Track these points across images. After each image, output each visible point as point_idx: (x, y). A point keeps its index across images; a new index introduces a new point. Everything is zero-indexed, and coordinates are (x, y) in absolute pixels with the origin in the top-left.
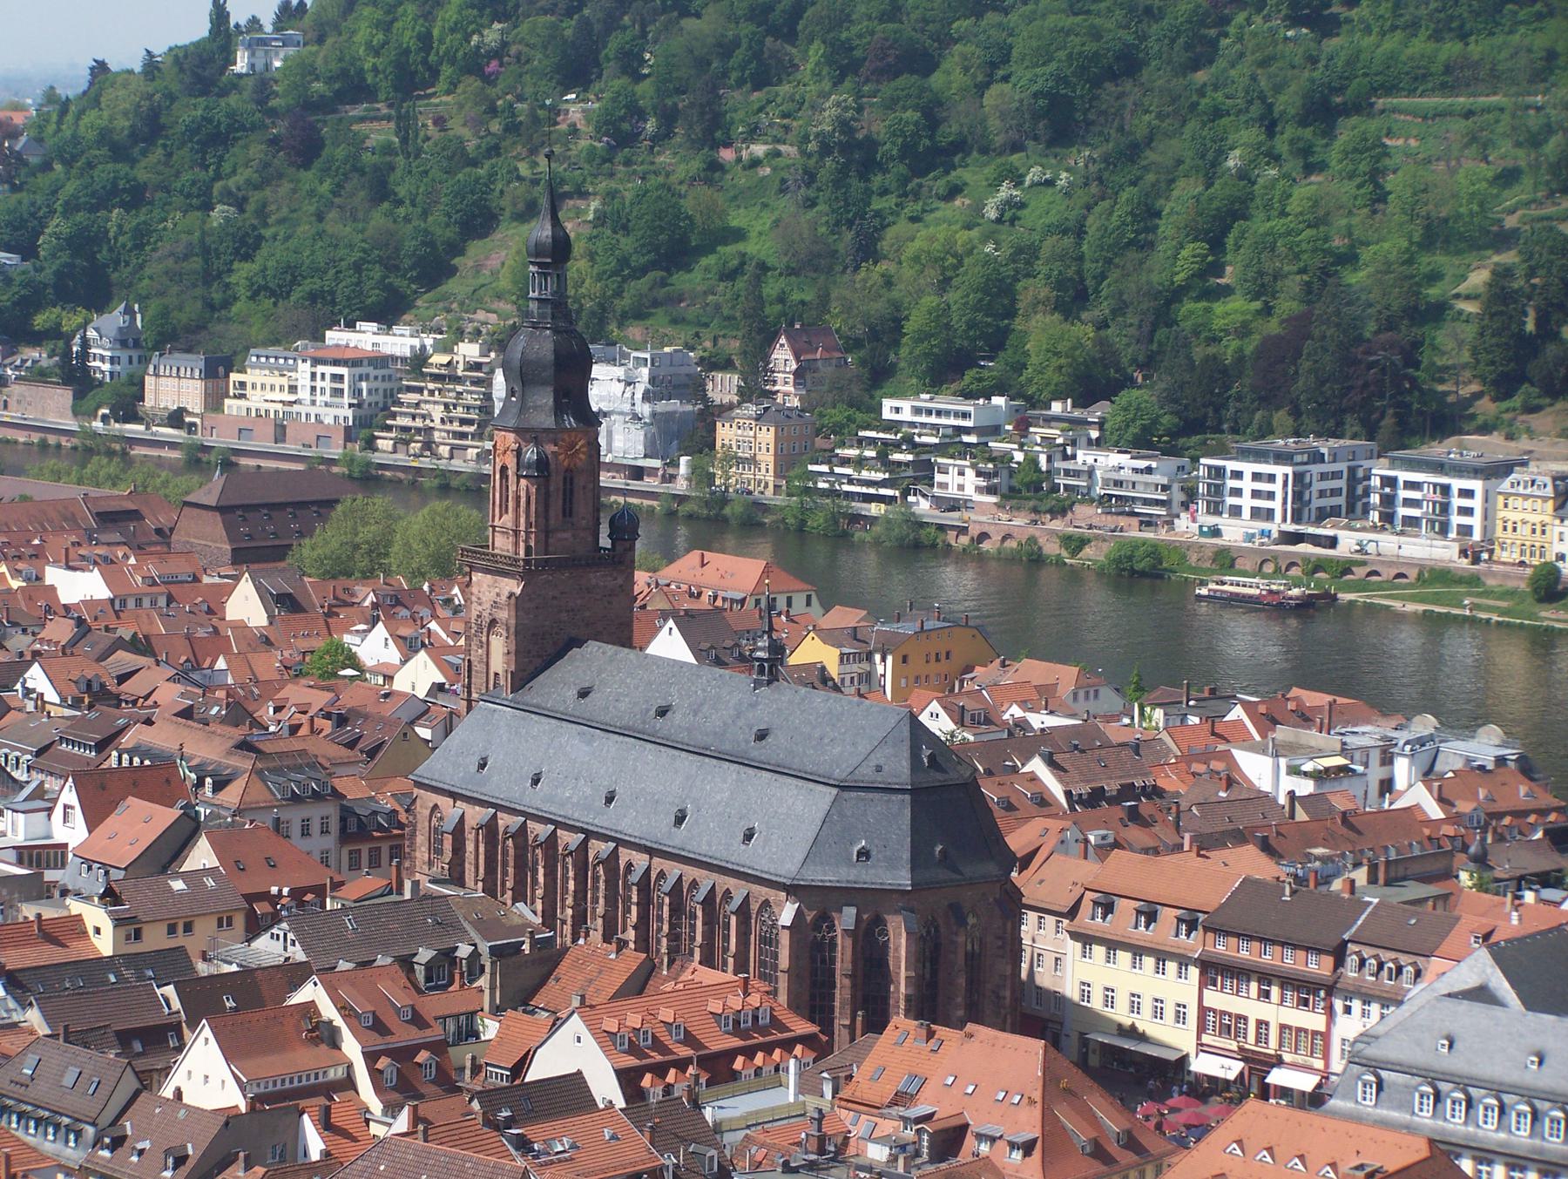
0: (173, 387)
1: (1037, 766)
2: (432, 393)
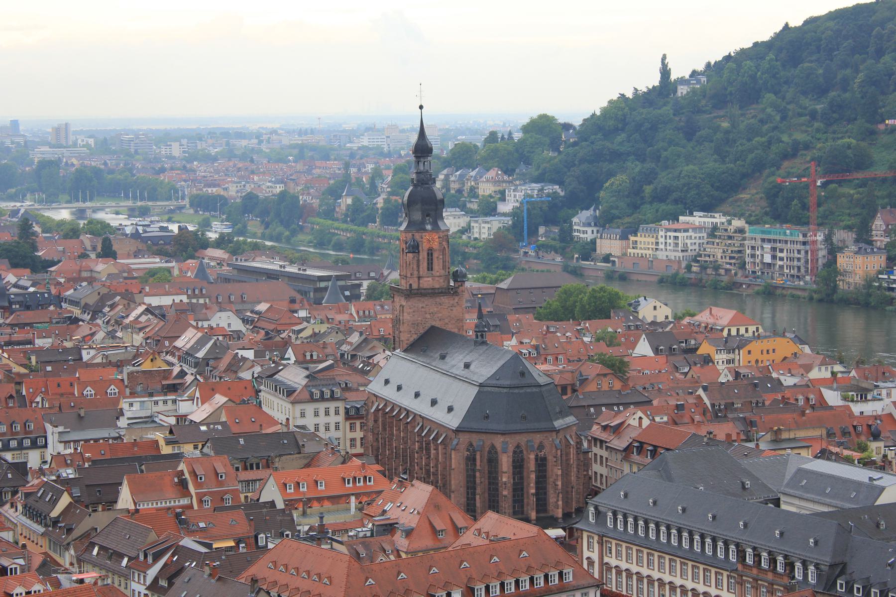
0: (609, 245)
1: (700, 392)
2: (718, 244)
